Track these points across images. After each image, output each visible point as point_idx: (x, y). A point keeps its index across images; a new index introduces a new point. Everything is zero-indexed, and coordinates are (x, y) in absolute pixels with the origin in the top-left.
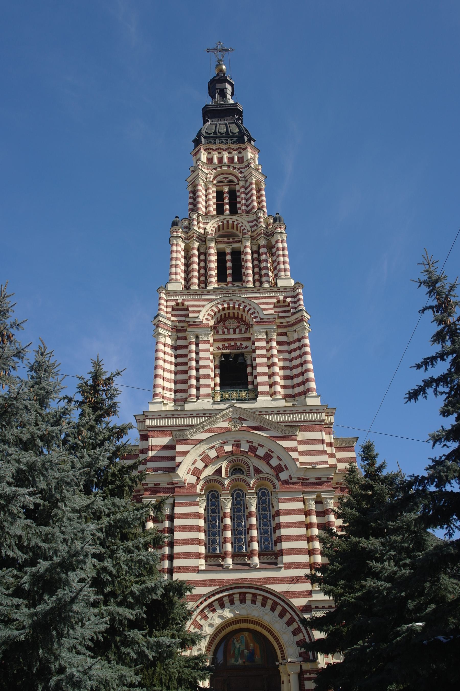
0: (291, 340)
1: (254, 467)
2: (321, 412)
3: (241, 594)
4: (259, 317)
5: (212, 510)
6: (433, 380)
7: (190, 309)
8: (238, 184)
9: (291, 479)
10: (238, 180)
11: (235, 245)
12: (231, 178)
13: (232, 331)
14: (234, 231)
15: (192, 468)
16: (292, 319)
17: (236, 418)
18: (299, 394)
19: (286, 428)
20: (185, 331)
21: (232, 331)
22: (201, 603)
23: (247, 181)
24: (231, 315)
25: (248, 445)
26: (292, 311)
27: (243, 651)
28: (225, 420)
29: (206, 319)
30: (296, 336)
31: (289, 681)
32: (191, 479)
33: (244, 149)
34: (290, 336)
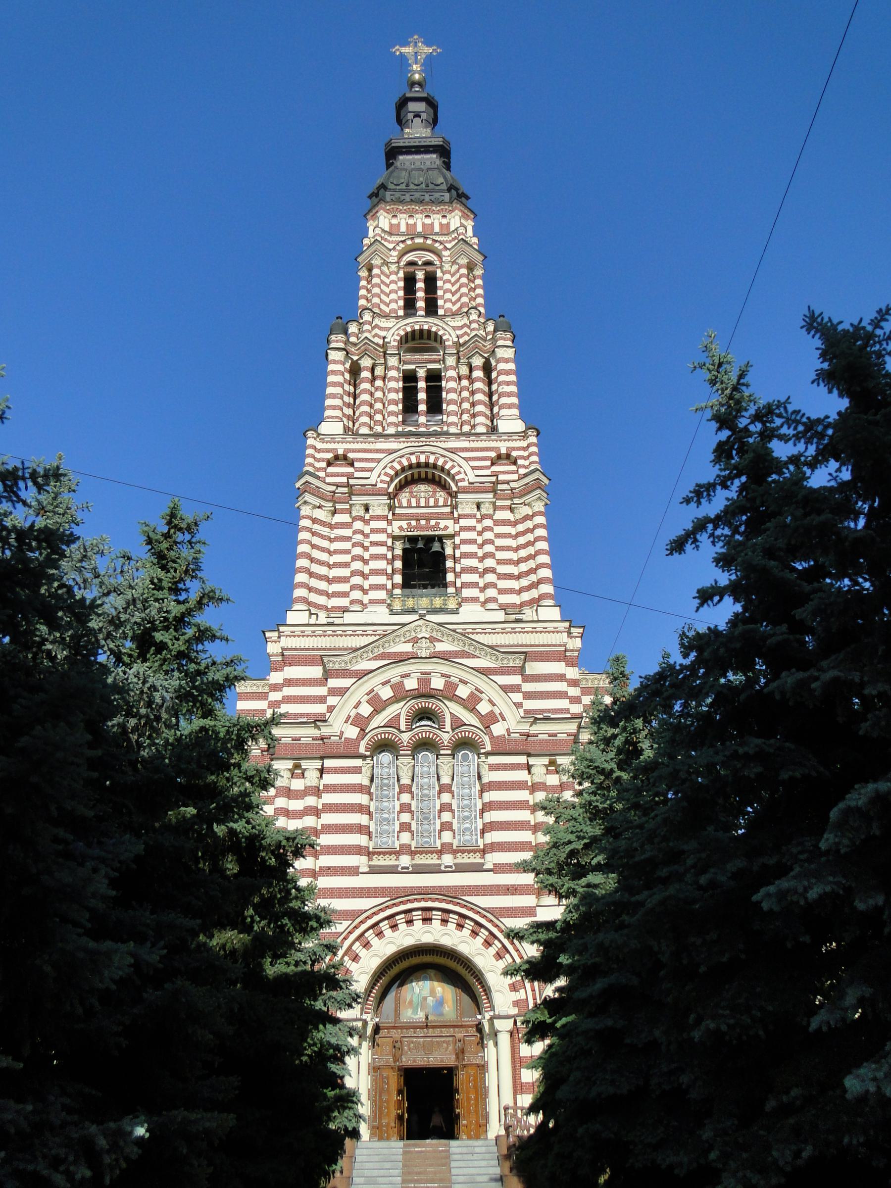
4: (466, 478)
6: (707, 520)
7: (357, 465)
9: (509, 735)
10: (441, 261)
12: (429, 258)
15: (353, 714)
17: (426, 638)
22: (362, 922)
27: (425, 998)
28: (408, 641)
32: (352, 732)
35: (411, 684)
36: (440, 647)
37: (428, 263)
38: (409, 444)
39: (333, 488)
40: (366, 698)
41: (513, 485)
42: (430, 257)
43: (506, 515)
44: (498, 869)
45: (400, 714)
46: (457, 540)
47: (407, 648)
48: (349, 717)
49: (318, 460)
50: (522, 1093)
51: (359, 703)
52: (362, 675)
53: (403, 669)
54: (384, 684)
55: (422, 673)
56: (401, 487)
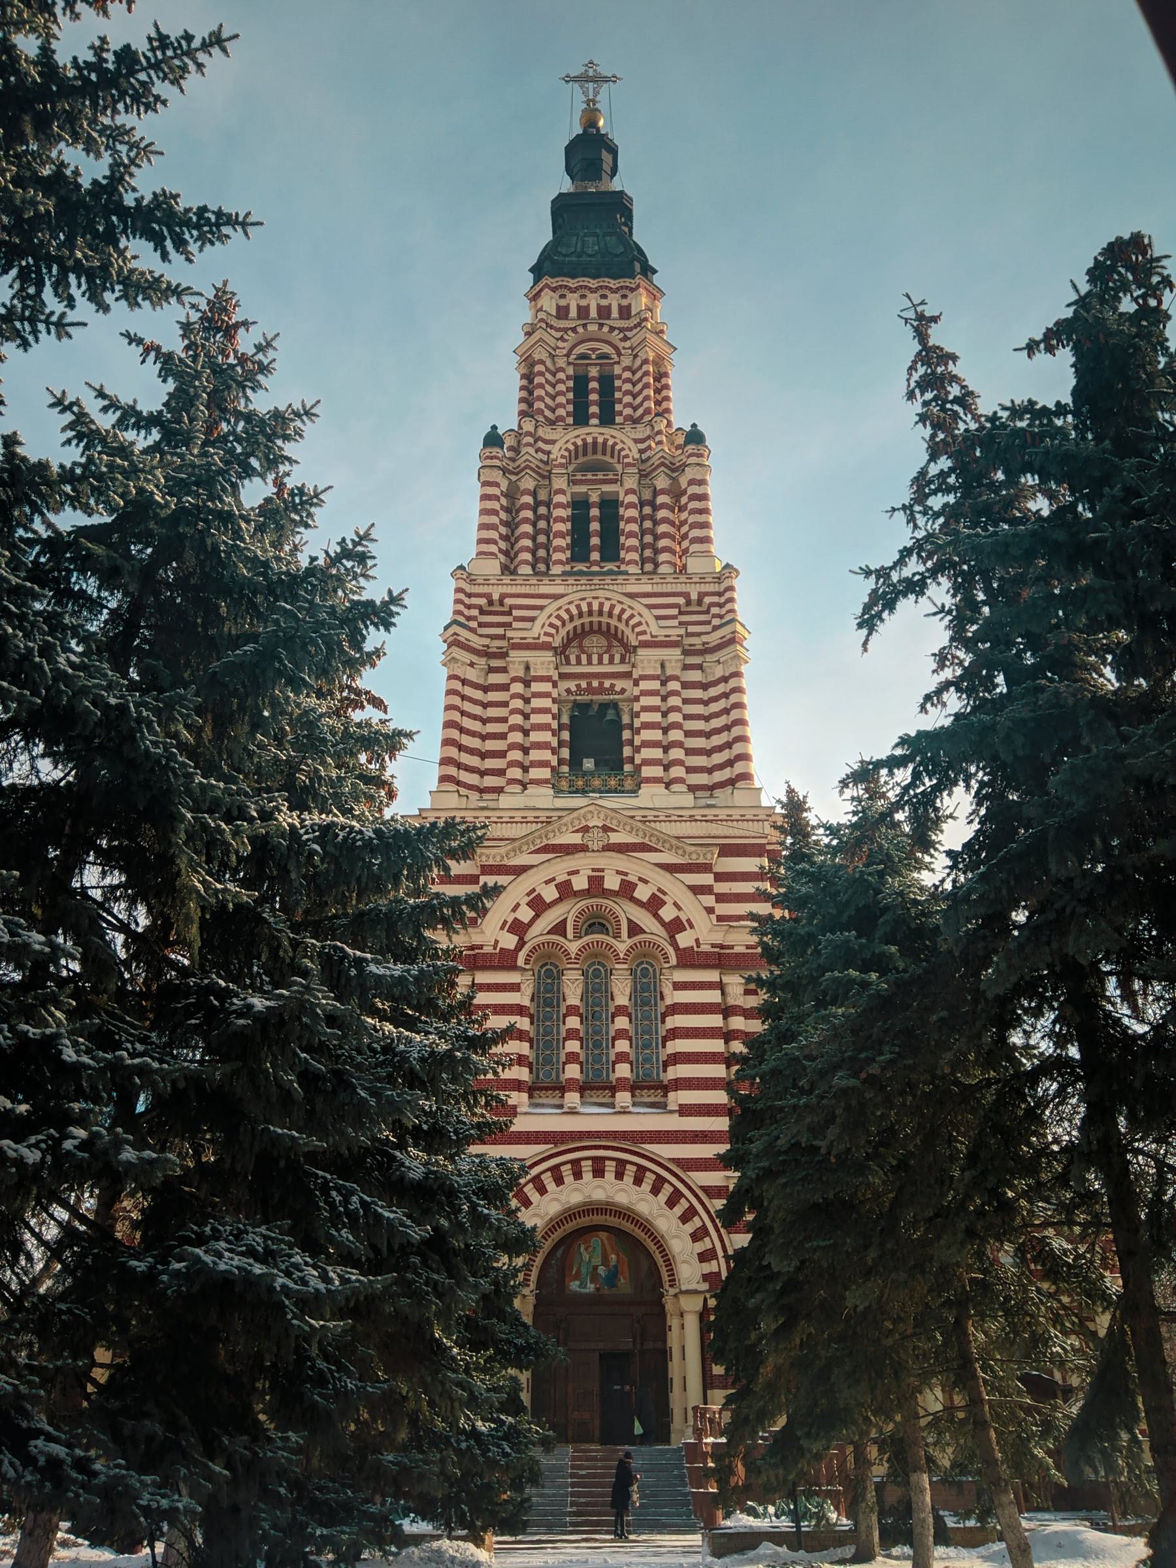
0: (711, 679)
1: (629, 920)
2: (763, 821)
3: (594, 1159)
5: (545, 999)
7: (515, 613)
8: (618, 363)
9: (698, 947)
10: (619, 354)
11: (606, 488)
12: (605, 350)
13: (595, 658)
14: (607, 458)
16: (714, 638)
18: (722, 785)
19: (693, 849)
20: (503, 655)
21: (595, 658)
23: (636, 356)
24: (596, 627)
25: (619, 878)
26: (716, 622)
27: (596, 1268)
28: (577, 831)
29: (546, 634)
30: (719, 672)
31: (683, 1327)
32: (509, 941)
33: (632, 290)
34: (708, 670)
35: (580, 883)
36: (615, 838)
37: (605, 356)
38: (579, 588)
39: (487, 641)
40: (528, 899)
41: (705, 638)
42: (607, 349)
43: (695, 676)
44: (686, 1110)
45: (565, 920)
46: (637, 707)
47: (576, 839)
48: (505, 922)
49: (469, 607)
50: (712, 1388)
51: (517, 906)
52: (520, 870)
53: (570, 863)
54: (547, 882)
55: (594, 870)
56: (569, 640)
